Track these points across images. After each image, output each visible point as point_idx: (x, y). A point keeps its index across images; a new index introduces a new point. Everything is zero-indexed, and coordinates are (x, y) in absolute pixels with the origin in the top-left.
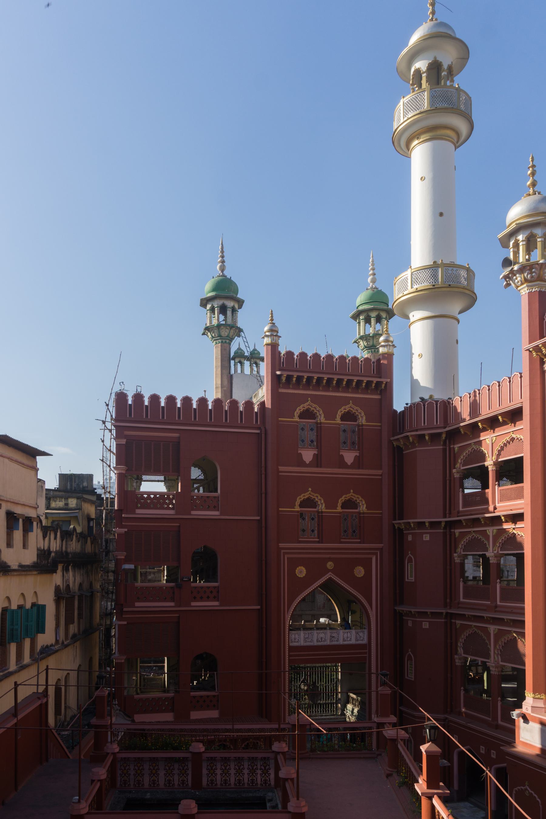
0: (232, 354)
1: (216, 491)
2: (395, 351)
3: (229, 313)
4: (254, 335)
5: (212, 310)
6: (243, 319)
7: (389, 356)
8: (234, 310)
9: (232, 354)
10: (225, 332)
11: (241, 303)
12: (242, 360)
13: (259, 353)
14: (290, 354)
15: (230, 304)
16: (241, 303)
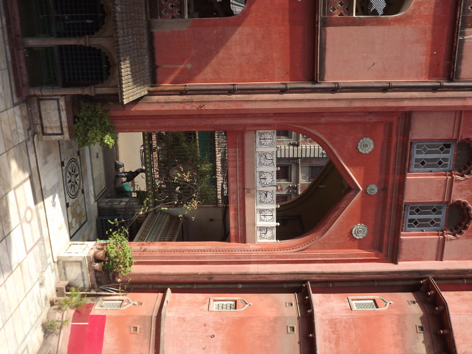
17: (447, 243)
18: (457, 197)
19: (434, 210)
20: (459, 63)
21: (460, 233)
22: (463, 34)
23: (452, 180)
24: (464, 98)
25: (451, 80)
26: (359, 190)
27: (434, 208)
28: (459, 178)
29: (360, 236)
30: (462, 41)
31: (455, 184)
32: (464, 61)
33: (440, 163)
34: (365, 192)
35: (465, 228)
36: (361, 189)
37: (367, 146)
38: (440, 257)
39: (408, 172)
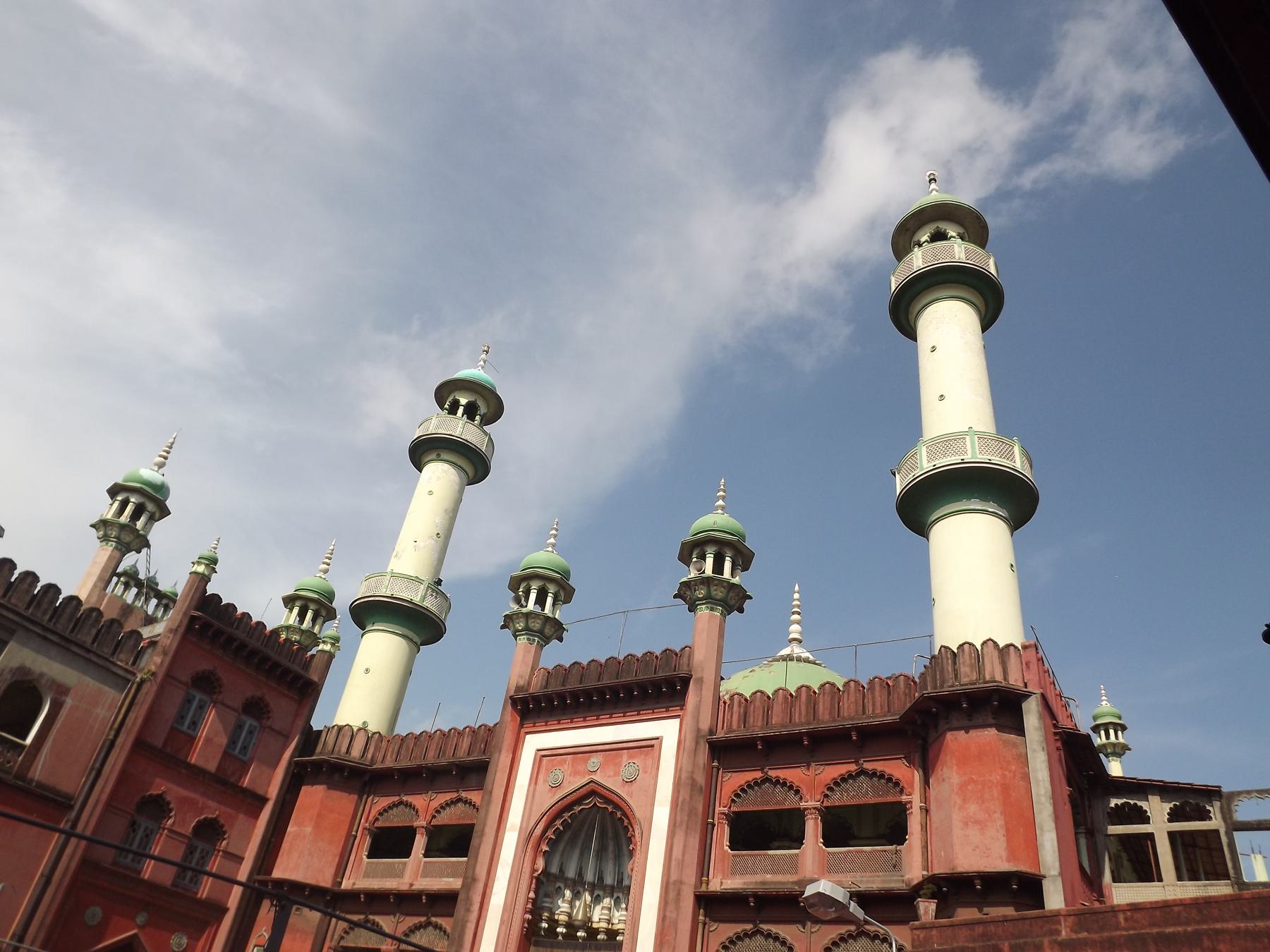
0: (120, 570)
1: (24, 738)
2: (338, 654)
3: (143, 519)
4: (169, 559)
5: (124, 504)
6: (159, 533)
7: (331, 656)
8: (152, 519)
9: (120, 570)
10: (127, 538)
11: (165, 512)
12: (132, 583)
13: (157, 584)
14: (216, 598)
15: (150, 507)
16: (165, 512)
17: (231, 850)
18: (188, 829)
19: (191, 853)
20: (58, 793)
21: (225, 833)
22: (32, 780)
23: (170, 830)
24: (97, 801)
25: (71, 807)
26: (135, 935)
27: (190, 851)
28: (170, 821)
29: (185, 941)
30: (39, 785)
31: (175, 828)
32: (59, 787)
33: (147, 836)
34: (140, 927)
35: (222, 826)
36: (135, 931)
37: (94, 914)
38: (240, 859)
39: (140, 873)
